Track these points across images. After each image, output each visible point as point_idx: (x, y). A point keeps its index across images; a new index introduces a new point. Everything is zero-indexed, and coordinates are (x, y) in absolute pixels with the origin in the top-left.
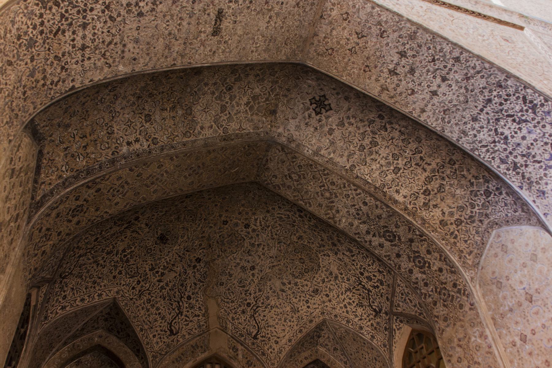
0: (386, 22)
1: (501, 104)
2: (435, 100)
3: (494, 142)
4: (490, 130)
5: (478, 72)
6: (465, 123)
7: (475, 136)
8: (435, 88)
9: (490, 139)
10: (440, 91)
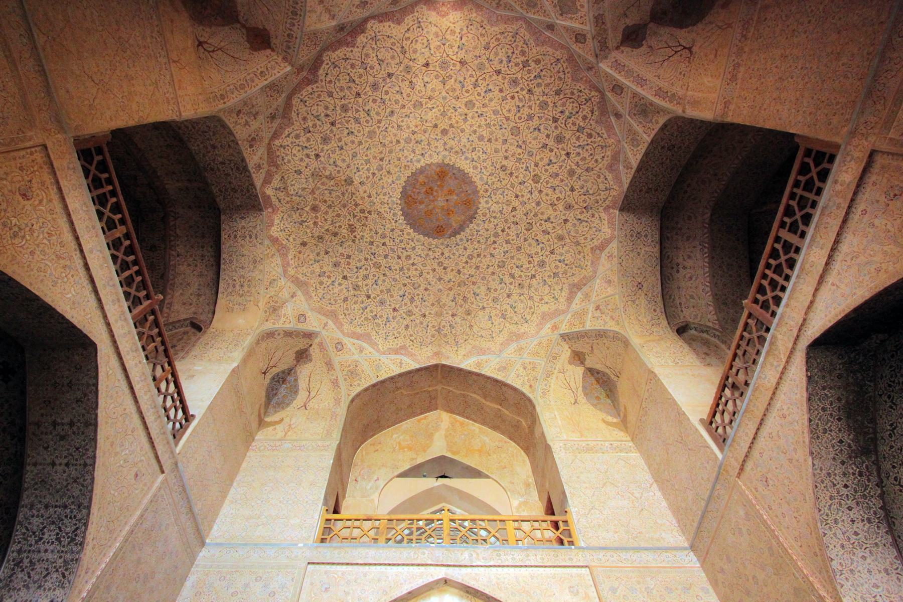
0: (88, 400)
1: (66, 517)
2: (49, 468)
3: (34, 533)
4: (42, 523)
5: (83, 486)
6: (40, 502)
7: (33, 516)
8: (57, 462)
9: (35, 528)
10: (58, 467)
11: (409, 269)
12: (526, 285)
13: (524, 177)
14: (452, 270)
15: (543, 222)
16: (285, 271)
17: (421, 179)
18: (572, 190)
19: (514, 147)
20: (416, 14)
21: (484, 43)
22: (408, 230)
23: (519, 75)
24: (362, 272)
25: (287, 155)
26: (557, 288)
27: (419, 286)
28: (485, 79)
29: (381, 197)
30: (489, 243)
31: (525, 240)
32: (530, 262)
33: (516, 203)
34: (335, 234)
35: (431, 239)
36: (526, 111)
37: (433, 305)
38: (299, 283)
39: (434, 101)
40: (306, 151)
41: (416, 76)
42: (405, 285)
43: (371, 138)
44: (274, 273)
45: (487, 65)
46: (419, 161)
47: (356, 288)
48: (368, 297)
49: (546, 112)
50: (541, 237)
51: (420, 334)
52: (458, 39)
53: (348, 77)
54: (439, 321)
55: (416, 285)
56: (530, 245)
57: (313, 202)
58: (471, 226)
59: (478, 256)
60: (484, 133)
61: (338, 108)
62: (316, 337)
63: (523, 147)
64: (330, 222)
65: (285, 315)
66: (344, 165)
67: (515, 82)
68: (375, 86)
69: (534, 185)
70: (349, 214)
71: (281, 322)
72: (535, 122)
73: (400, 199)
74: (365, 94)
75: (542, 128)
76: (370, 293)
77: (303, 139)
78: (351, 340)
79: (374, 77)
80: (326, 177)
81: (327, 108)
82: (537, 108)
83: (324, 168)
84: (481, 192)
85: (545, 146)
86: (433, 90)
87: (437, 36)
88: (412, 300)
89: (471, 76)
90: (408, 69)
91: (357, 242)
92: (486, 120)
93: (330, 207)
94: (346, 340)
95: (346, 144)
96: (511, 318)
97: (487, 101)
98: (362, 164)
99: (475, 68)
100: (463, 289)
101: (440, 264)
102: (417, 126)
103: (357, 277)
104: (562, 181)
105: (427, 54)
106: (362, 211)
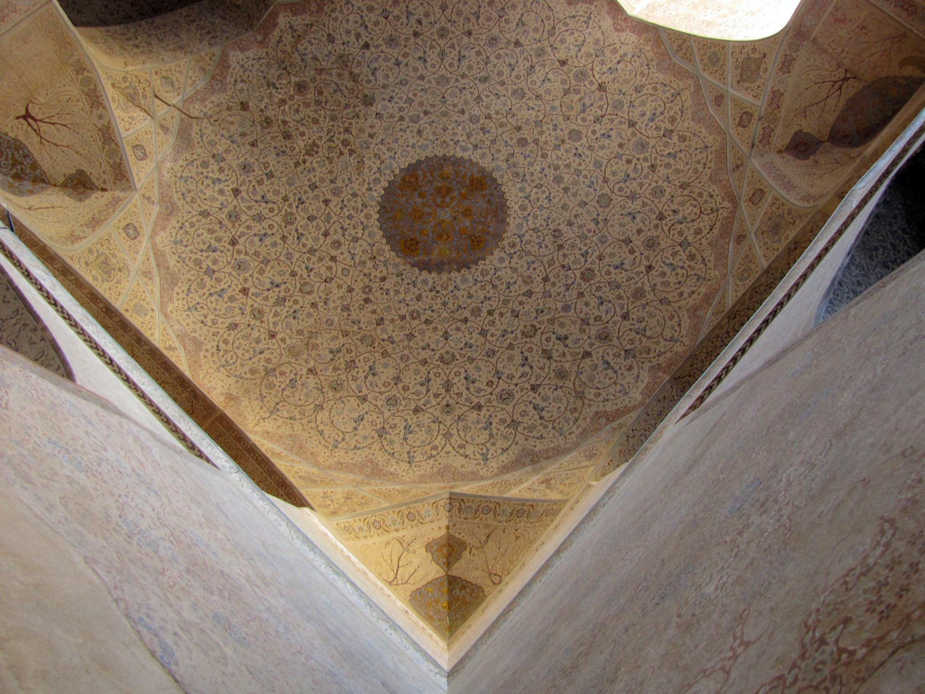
11: (321, 259)
12: (458, 412)
13: (574, 262)
14: (374, 312)
15: (554, 337)
16: (189, 100)
17: (448, 170)
18: (625, 317)
19: (589, 218)
20: (593, 7)
21: (638, 83)
22: (374, 211)
23: (652, 142)
24: (263, 209)
25: (341, 12)
26: (501, 444)
27: (310, 293)
28: (612, 121)
29: (384, 148)
30: (456, 315)
31: (511, 347)
32: (490, 383)
33: (538, 287)
34: (287, 136)
35: (388, 247)
36: (634, 186)
37: (300, 332)
38: (184, 135)
39: (540, 102)
40: (362, 30)
41: (544, 66)
42: (293, 274)
43: (438, 83)
44: (182, 80)
45: (626, 108)
46: (464, 149)
47: (234, 217)
48: (233, 243)
49: (656, 201)
50: (535, 358)
51: (240, 352)
52: (615, 61)
53: (476, 9)
54: (285, 359)
55: (307, 288)
56: (511, 359)
57: (308, 80)
58: (454, 274)
59: (427, 322)
60: (566, 177)
61: (437, 26)
62: (123, 190)
63: (601, 225)
64: (297, 117)
65: (133, 118)
66: (381, 80)
67: (643, 146)
68: (493, 41)
69: (578, 280)
70: (329, 131)
71: (121, 114)
72: (636, 206)
73: (401, 170)
74: (477, 39)
75: (639, 217)
76: (241, 240)
77: (373, 17)
78: (151, 254)
79: (501, 32)
80: (351, 73)
81: (427, 15)
82: (649, 191)
83: (359, 63)
84: (505, 242)
85: (628, 241)
86: (548, 92)
87: (597, 42)
88: (281, 301)
89: (601, 107)
90: (541, 52)
91: (299, 169)
92: (580, 164)
93: (318, 103)
94: (145, 240)
95: (407, 65)
96: (391, 442)
97: (597, 146)
98: (401, 98)
99: (611, 102)
100: (362, 349)
101: (367, 289)
102: (497, 113)
103: (249, 208)
104: (620, 297)
105: (573, 53)
106: (345, 143)
